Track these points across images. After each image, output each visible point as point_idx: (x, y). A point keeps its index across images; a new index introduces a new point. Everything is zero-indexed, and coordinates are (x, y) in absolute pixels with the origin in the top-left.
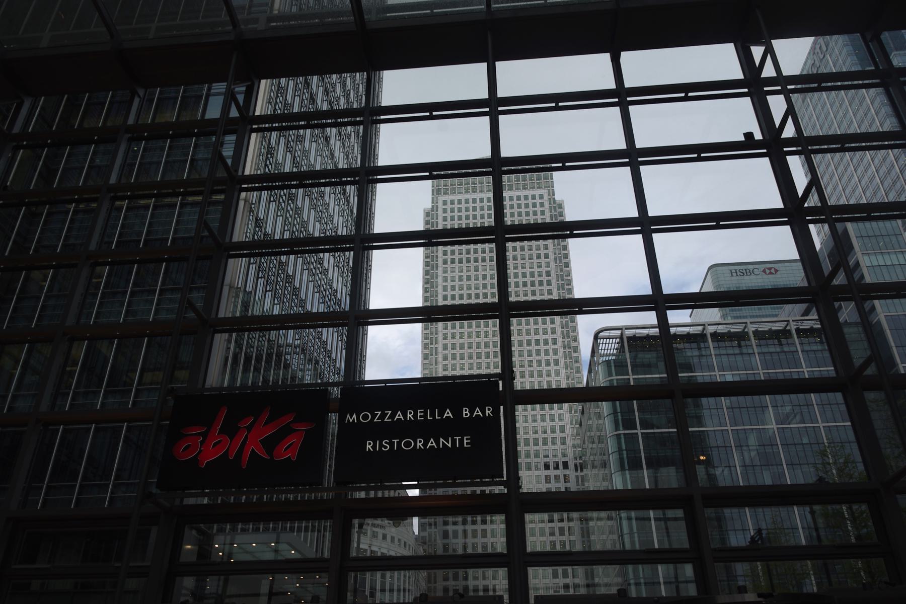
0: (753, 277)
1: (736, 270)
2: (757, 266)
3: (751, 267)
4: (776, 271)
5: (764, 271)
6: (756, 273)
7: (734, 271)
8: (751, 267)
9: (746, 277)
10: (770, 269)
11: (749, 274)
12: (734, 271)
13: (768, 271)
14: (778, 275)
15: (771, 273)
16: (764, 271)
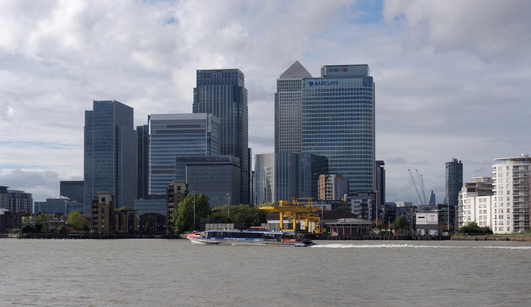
0: (338, 72)
1: (331, 69)
2: (340, 67)
3: (337, 68)
4: (347, 70)
5: (342, 70)
6: (339, 71)
7: (330, 69)
8: (337, 68)
9: (335, 72)
10: (345, 69)
11: (336, 71)
12: (330, 69)
13: (344, 70)
14: (347, 72)
15: (345, 71)
16: (342, 70)
